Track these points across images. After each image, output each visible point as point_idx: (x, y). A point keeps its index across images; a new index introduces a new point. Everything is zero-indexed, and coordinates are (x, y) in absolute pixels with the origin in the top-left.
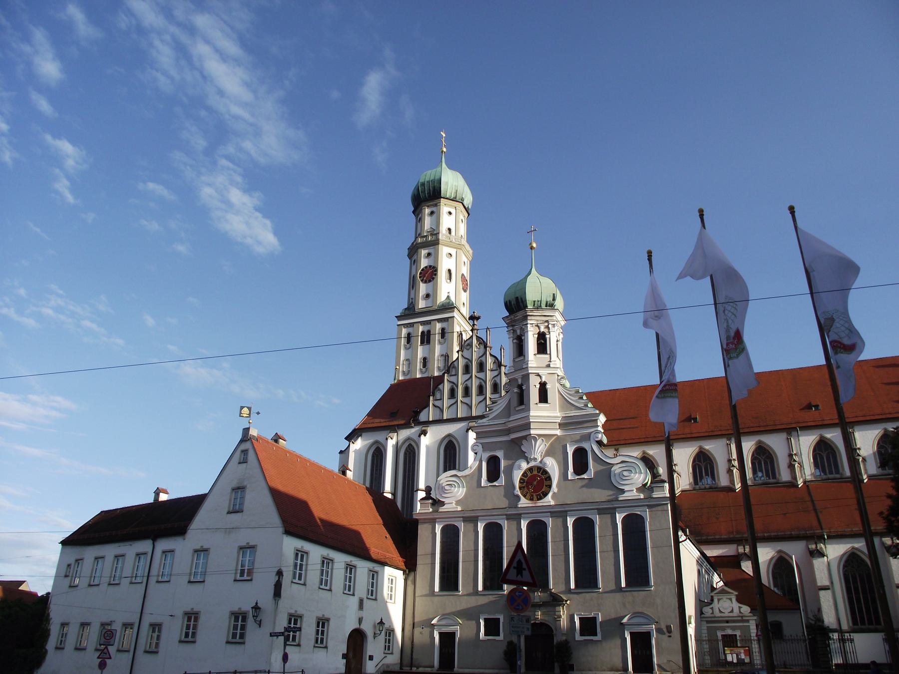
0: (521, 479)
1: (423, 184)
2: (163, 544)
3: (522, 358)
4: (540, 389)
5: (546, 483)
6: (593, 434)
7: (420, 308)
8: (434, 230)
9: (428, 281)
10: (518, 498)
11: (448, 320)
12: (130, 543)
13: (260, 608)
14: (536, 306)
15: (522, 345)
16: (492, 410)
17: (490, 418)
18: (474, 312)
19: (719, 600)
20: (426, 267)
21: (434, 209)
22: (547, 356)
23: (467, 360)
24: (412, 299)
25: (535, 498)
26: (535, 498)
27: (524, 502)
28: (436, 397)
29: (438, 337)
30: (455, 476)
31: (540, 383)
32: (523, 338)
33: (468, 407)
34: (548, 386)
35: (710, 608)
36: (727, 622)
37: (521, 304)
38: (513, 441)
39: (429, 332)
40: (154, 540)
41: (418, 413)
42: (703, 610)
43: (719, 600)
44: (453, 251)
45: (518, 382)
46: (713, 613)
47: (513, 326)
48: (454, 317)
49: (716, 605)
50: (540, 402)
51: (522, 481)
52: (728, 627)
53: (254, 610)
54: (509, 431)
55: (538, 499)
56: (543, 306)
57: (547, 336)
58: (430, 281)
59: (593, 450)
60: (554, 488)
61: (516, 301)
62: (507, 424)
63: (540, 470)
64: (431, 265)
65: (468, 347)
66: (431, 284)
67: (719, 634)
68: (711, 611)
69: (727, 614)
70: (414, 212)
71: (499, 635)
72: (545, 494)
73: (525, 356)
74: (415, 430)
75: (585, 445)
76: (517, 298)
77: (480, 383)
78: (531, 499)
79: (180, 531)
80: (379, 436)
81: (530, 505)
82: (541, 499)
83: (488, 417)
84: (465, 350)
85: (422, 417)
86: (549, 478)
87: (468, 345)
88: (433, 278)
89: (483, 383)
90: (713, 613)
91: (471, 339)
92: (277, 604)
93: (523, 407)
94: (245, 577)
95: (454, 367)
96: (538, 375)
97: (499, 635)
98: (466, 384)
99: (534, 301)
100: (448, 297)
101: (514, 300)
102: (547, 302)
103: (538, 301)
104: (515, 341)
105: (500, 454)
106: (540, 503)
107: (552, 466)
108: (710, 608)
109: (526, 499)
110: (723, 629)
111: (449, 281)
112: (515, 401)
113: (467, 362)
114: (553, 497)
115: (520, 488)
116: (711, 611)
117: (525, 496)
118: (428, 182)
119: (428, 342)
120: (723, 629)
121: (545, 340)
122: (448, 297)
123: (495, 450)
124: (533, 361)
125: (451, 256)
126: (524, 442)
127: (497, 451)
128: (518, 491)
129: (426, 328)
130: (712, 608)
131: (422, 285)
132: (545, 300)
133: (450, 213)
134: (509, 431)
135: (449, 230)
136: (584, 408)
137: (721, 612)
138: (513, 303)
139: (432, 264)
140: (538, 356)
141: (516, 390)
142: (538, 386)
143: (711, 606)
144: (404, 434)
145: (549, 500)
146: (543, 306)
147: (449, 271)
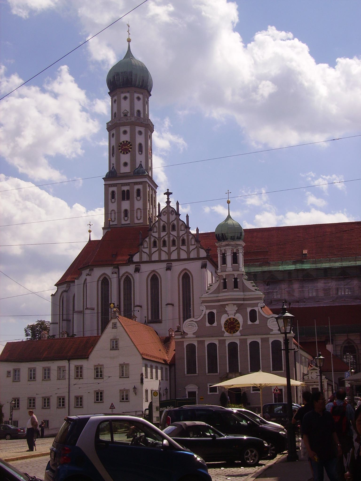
0: (225, 323)
1: (118, 74)
2: (74, 363)
3: (225, 265)
4: (234, 281)
5: (237, 325)
6: (259, 303)
7: (121, 172)
8: (128, 112)
9: (125, 153)
10: (224, 332)
11: (142, 183)
12: (52, 362)
13: (136, 388)
14: (232, 238)
15: (225, 258)
16: (210, 289)
17: (209, 293)
18: (168, 190)
19: (311, 373)
20: (123, 142)
21: (128, 95)
22: (237, 265)
23: (164, 223)
24: (113, 164)
25: (232, 332)
26: (232, 332)
27: (226, 334)
28: (144, 247)
30: (193, 321)
31: (234, 278)
32: (226, 255)
33: (166, 254)
34: (238, 280)
35: (307, 377)
36: (315, 382)
37: (224, 237)
38: (221, 305)
39: (128, 191)
40: (69, 361)
41: (132, 256)
42: (304, 377)
43: (311, 373)
44: (142, 130)
45: (223, 277)
46: (308, 378)
47: (220, 247)
48: (146, 182)
49: (310, 375)
50: (234, 288)
51: (225, 324)
52: (315, 384)
53: (134, 389)
54: (219, 301)
55: (234, 333)
56: (236, 238)
57: (238, 255)
58: (127, 153)
59: (259, 311)
60: (241, 328)
61: (222, 235)
62: (218, 297)
63: (234, 320)
64: (127, 140)
65: (165, 213)
66: (129, 154)
67: (311, 387)
68: (308, 378)
69: (314, 379)
70: (109, 93)
71: (210, 392)
72: (237, 331)
73: (227, 265)
74: (131, 269)
75: (256, 309)
76: (222, 234)
77: (173, 238)
78: (230, 333)
79: (86, 357)
80: (108, 271)
81: (230, 335)
82: (235, 332)
83: (208, 292)
84: (162, 215)
85: (136, 258)
86: (239, 323)
87: (164, 212)
89: (175, 238)
90: (308, 378)
91: (166, 208)
92: (142, 386)
93: (226, 290)
94: (124, 376)
95: (155, 226)
96: (234, 275)
97: (210, 392)
98: (164, 239)
99: (231, 237)
100: (141, 165)
101: (221, 234)
102: (237, 237)
103: (233, 236)
104: (221, 256)
105: (215, 311)
106: (234, 335)
107: (239, 318)
108: (307, 377)
109: (228, 333)
110: (312, 385)
111: (140, 153)
112: (222, 286)
113: (164, 224)
114: (240, 332)
115: (225, 328)
116: (308, 378)
117: (227, 331)
118: (121, 73)
120: (312, 385)
121: (236, 256)
122: (141, 165)
123: (212, 309)
124: (230, 268)
125: (141, 134)
126: (227, 306)
127: (213, 310)
128: (223, 329)
129: (125, 188)
130: (308, 377)
131: (122, 156)
132: (237, 236)
134: (219, 301)
135: (139, 111)
136: (255, 291)
137: (312, 378)
138: (220, 236)
139: (129, 140)
140: (233, 265)
141: (222, 281)
142: (233, 280)
143: (308, 376)
144: (123, 270)
145: (238, 333)
146: (236, 238)
147: (140, 145)
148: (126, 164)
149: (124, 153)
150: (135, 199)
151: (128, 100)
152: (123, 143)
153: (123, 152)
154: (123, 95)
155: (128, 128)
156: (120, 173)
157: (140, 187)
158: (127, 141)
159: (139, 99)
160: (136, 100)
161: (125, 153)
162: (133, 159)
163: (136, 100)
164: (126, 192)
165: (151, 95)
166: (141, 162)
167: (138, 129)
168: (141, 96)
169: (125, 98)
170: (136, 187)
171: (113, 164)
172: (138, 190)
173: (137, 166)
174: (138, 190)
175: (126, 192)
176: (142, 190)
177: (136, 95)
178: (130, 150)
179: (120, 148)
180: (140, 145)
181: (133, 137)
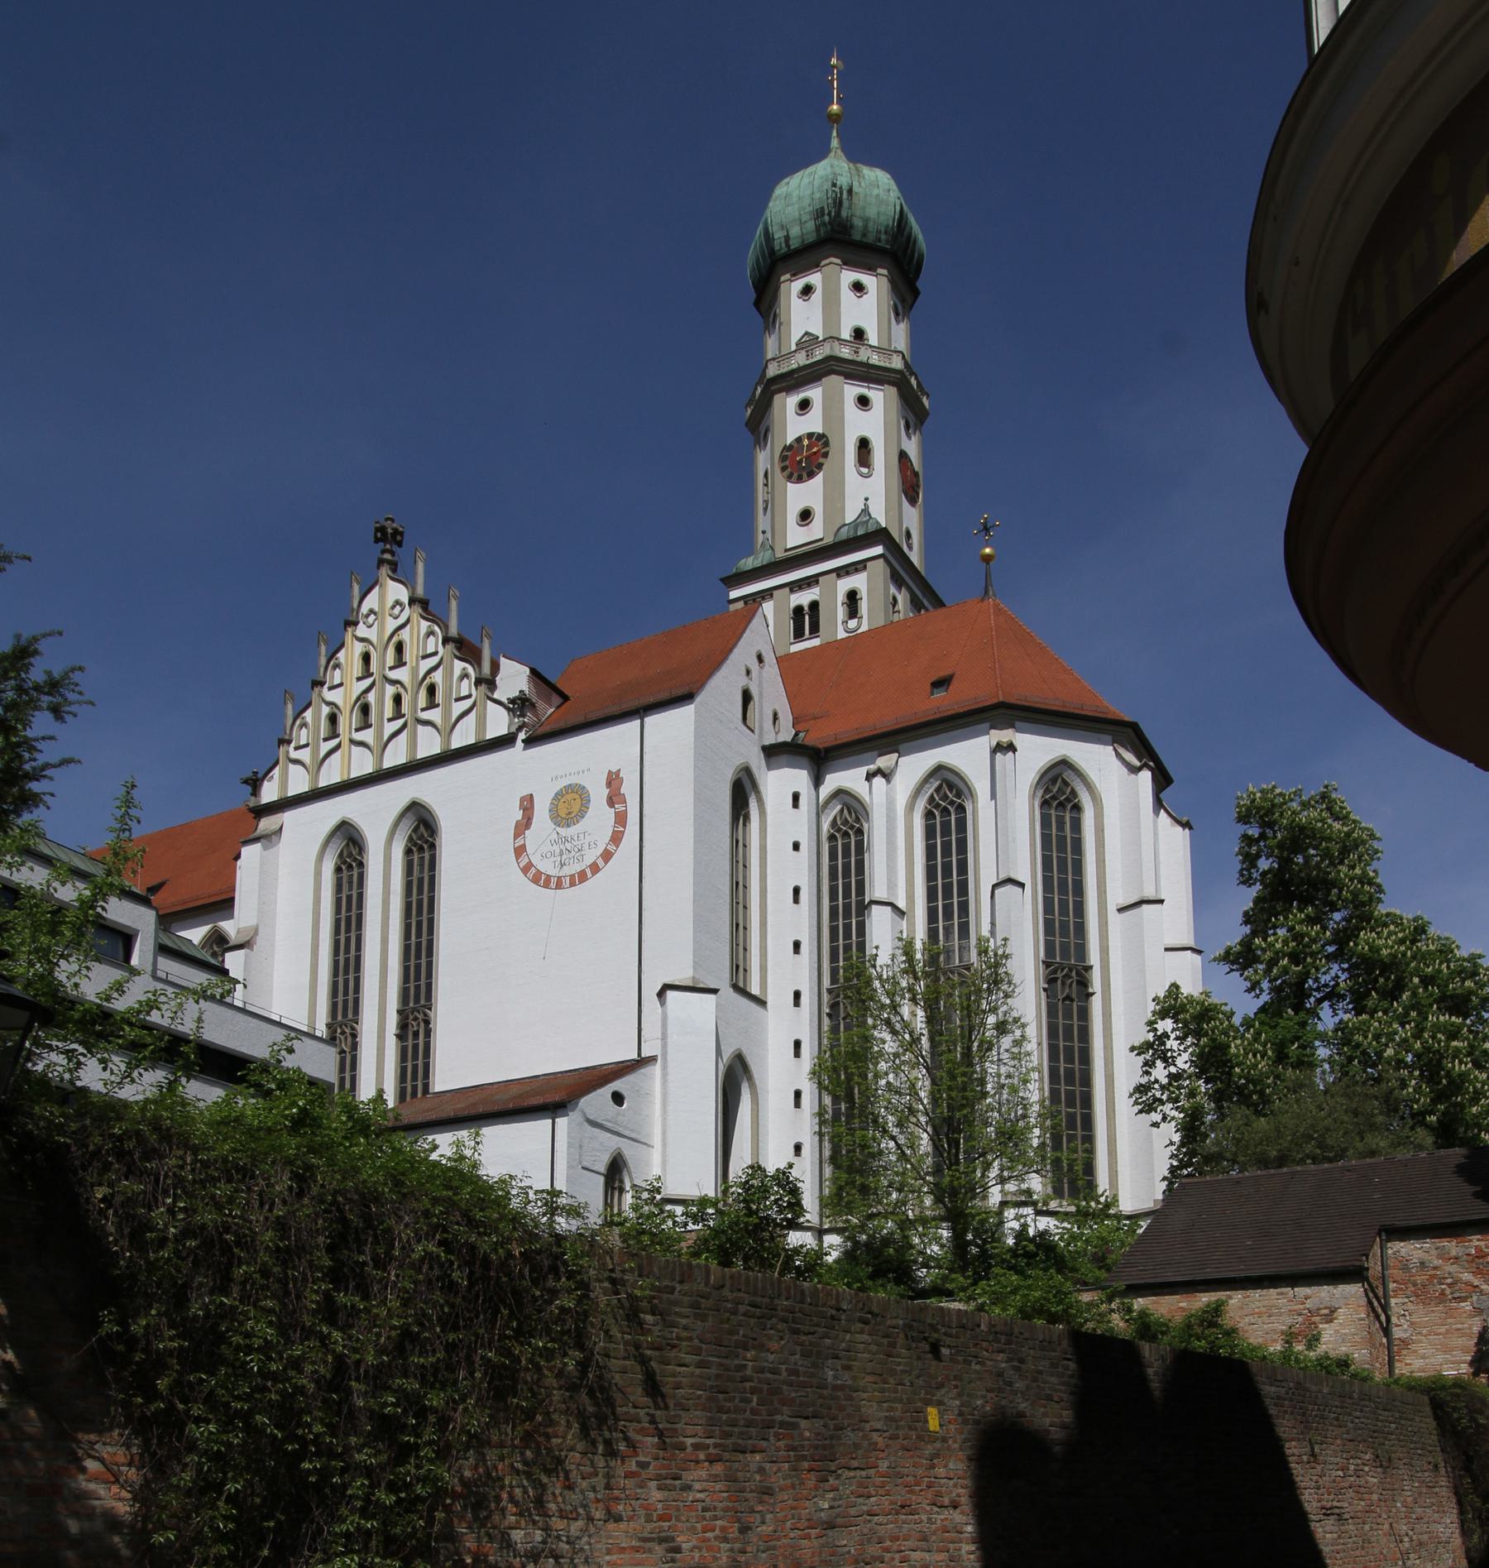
9: (805, 475)
20: (799, 440)
21: (815, 279)
24: (764, 532)
29: (841, 612)
39: (814, 605)
58: (811, 475)
70: (757, 304)
88: (820, 466)
100: (865, 511)
111: (865, 470)
119: (815, 629)
122: (865, 511)
129: (804, 598)
131: (791, 487)
133: (858, 287)
139: (819, 430)
147: (864, 445)
148: (806, 516)
149: (800, 480)
150: (840, 628)
151: (817, 296)
152: (796, 445)
153: (796, 475)
154: (798, 285)
155: (815, 393)
156: (786, 550)
157: (858, 581)
158: (810, 436)
159: (858, 287)
160: (847, 295)
161: (805, 475)
162: (835, 495)
163: (847, 295)
164: (806, 608)
165: (916, 293)
166: (866, 499)
167: (852, 391)
168: (868, 280)
169: (807, 290)
170: (844, 585)
171: (764, 532)
172: (852, 597)
173: (850, 518)
174: (852, 597)
175: (806, 608)
176: (863, 593)
177: (849, 276)
178: (821, 460)
179: (787, 463)
180: (864, 445)
181: (833, 412)
